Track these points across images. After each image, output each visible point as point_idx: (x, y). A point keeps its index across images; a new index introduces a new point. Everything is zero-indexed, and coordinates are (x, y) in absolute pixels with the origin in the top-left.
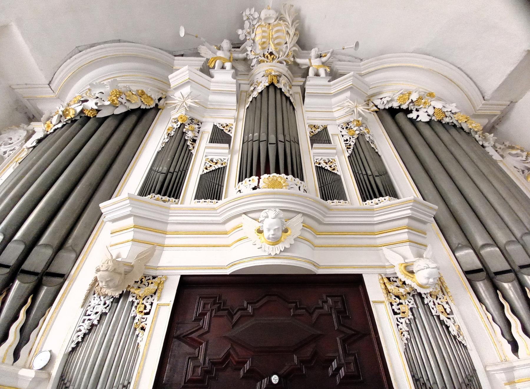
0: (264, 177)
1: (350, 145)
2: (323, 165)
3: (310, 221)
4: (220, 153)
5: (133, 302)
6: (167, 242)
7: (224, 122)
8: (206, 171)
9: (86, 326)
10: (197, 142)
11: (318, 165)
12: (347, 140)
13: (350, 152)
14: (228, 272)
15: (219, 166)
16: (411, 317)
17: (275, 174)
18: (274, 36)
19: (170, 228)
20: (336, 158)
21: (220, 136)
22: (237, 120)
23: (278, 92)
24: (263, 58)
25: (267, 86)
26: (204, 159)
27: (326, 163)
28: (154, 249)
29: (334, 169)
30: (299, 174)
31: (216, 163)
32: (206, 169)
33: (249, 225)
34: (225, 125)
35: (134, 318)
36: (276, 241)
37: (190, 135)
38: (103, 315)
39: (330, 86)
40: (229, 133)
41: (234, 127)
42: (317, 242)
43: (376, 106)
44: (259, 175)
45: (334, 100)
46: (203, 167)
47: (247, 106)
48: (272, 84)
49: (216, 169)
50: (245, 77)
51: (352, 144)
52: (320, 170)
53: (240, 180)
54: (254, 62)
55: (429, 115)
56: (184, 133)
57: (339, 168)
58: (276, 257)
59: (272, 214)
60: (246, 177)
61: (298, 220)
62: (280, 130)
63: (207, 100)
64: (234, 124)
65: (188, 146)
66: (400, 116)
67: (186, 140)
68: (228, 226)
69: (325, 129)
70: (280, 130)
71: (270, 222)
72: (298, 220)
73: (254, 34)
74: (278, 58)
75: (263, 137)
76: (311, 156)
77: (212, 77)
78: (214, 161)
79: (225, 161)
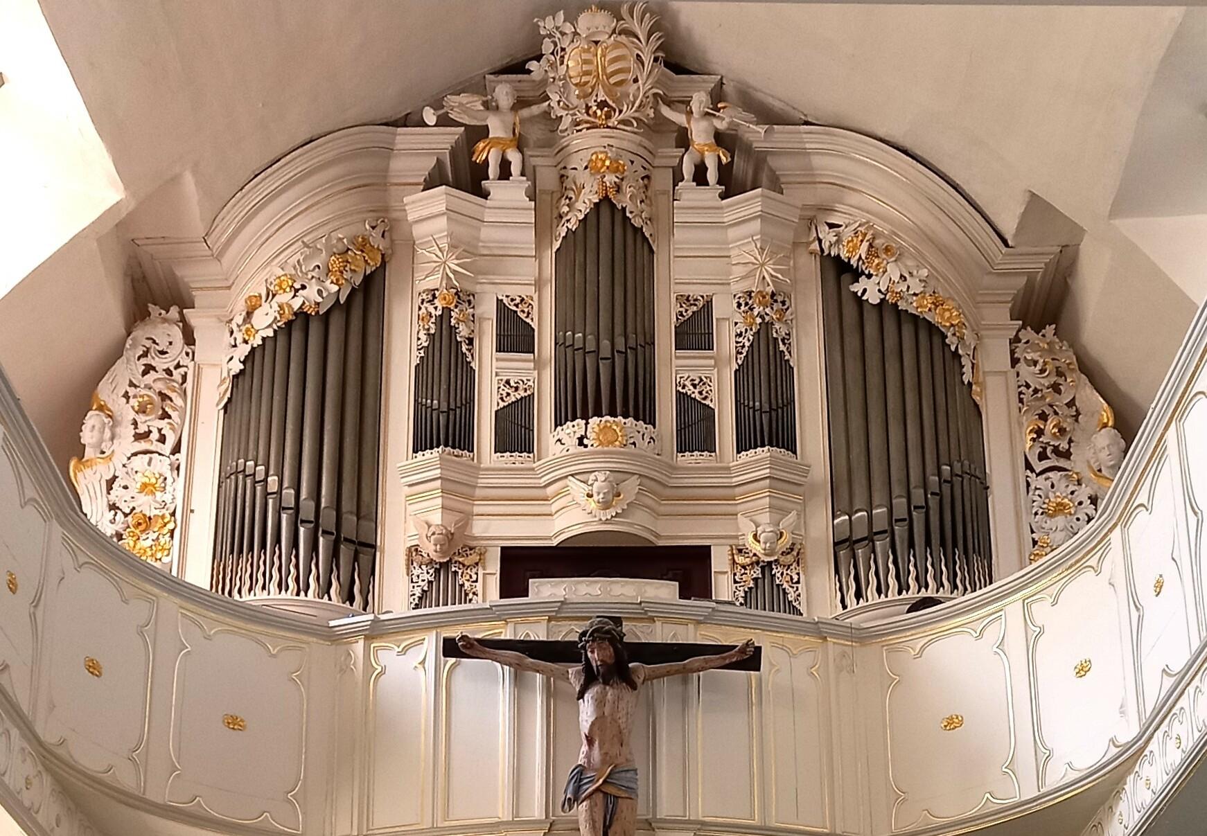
0: (594, 421)
1: (743, 347)
2: (689, 389)
3: (646, 481)
4: (518, 367)
5: (456, 572)
6: (476, 510)
7: (515, 292)
8: (502, 404)
9: (418, 592)
10: (476, 343)
11: (680, 389)
12: (740, 335)
13: (740, 362)
14: (555, 543)
15: (523, 394)
16: (751, 585)
17: (608, 418)
18: (609, 70)
19: (479, 493)
20: (714, 374)
21: (515, 336)
22: (539, 284)
23: (618, 218)
24: (586, 117)
25: (595, 204)
26: (495, 380)
27: (695, 386)
28: (466, 519)
29: (705, 398)
30: (644, 411)
31: (517, 389)
32: (502, 399)
33: (577, 488)
34: (518, 301)
35: (462, 586)
36: (606, 505)
37: (463, 331)
38: (430, 582)
39: (721, 208)
40: (528, 320)
41: (535, 304)
42: (662, 509)
43: (820, 241)
44: (586, 417)
45: (732, 233)
46: (496, 398)
47: (557, 245)
48: (606, 199)
49: (517, 401)
50: (546, 151)
51: (747, 344)
52: (682, 398)
53: (558, 423)
54: (566, 123)
55: (880, 291)
56: (452, 330)
57: (714, 395)
58: (607, 522)
59: (601, 477)
60: (566, 420)
61: (633, 482)
62: (618, 329)
63: (478, 240)
64: (536, 297)
65: (463, 354)
66: (846, 278)
67: (458, 344)
68: (550, 490)
69: (708, 304)
70: (618, 329)
71: (599, 483)
72: (633, 482)
73: (564, 67)
74: (621, 112)
75: (591, 346)
76: (674, 370)
77: (485, 195)
78: (512, 384)
79: (530, 383)
